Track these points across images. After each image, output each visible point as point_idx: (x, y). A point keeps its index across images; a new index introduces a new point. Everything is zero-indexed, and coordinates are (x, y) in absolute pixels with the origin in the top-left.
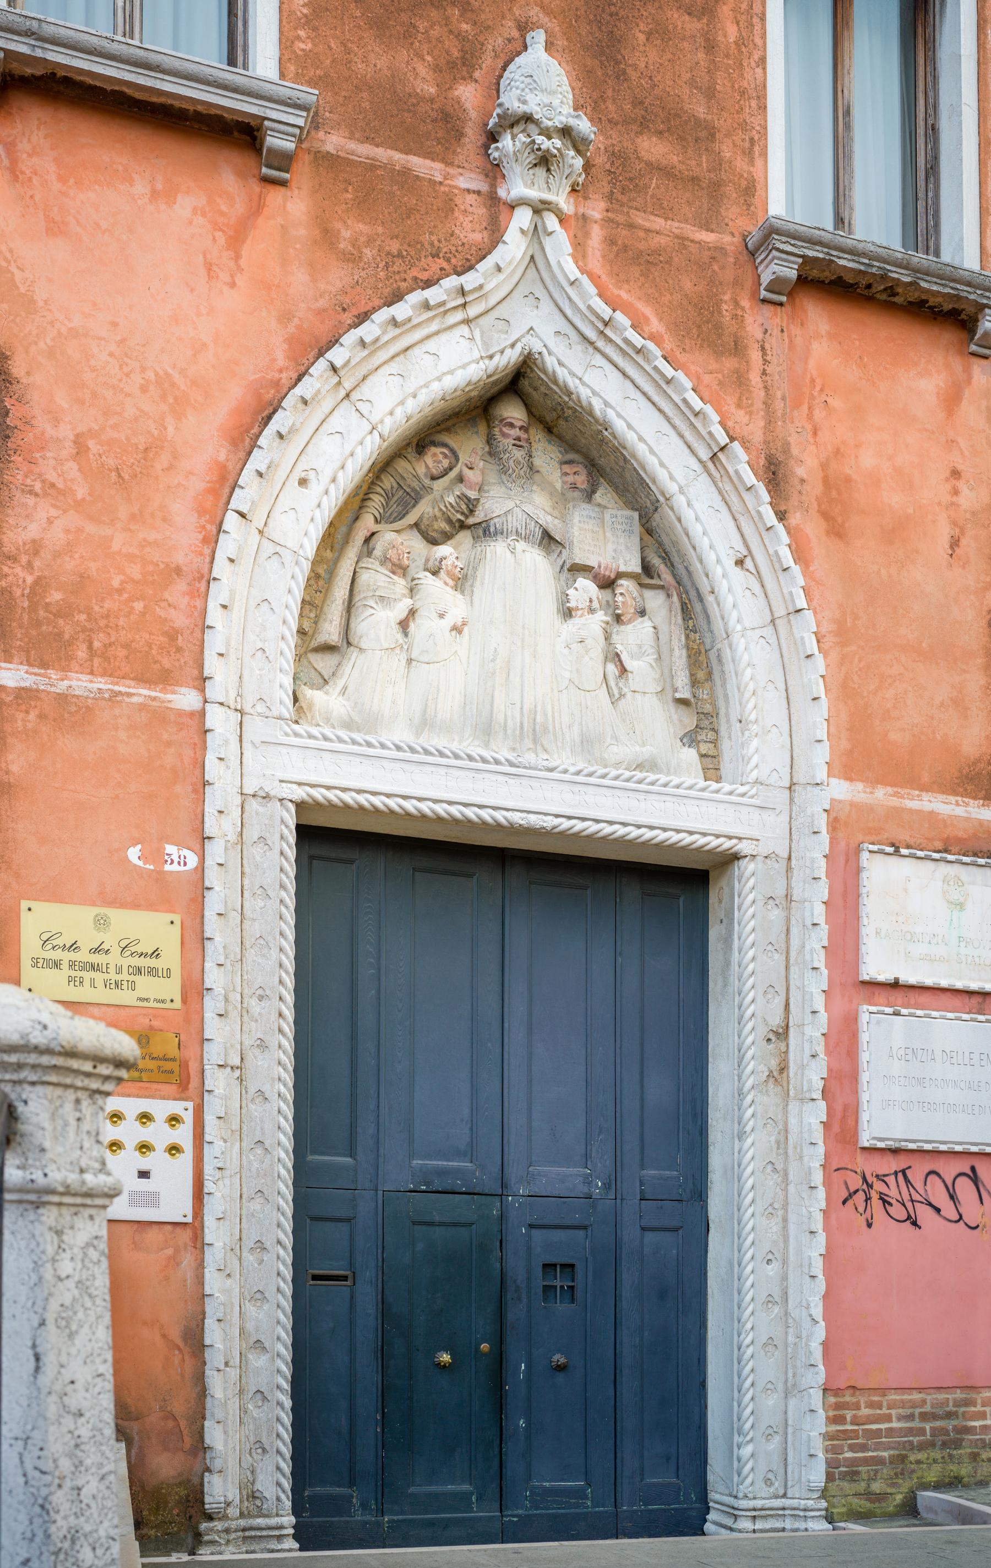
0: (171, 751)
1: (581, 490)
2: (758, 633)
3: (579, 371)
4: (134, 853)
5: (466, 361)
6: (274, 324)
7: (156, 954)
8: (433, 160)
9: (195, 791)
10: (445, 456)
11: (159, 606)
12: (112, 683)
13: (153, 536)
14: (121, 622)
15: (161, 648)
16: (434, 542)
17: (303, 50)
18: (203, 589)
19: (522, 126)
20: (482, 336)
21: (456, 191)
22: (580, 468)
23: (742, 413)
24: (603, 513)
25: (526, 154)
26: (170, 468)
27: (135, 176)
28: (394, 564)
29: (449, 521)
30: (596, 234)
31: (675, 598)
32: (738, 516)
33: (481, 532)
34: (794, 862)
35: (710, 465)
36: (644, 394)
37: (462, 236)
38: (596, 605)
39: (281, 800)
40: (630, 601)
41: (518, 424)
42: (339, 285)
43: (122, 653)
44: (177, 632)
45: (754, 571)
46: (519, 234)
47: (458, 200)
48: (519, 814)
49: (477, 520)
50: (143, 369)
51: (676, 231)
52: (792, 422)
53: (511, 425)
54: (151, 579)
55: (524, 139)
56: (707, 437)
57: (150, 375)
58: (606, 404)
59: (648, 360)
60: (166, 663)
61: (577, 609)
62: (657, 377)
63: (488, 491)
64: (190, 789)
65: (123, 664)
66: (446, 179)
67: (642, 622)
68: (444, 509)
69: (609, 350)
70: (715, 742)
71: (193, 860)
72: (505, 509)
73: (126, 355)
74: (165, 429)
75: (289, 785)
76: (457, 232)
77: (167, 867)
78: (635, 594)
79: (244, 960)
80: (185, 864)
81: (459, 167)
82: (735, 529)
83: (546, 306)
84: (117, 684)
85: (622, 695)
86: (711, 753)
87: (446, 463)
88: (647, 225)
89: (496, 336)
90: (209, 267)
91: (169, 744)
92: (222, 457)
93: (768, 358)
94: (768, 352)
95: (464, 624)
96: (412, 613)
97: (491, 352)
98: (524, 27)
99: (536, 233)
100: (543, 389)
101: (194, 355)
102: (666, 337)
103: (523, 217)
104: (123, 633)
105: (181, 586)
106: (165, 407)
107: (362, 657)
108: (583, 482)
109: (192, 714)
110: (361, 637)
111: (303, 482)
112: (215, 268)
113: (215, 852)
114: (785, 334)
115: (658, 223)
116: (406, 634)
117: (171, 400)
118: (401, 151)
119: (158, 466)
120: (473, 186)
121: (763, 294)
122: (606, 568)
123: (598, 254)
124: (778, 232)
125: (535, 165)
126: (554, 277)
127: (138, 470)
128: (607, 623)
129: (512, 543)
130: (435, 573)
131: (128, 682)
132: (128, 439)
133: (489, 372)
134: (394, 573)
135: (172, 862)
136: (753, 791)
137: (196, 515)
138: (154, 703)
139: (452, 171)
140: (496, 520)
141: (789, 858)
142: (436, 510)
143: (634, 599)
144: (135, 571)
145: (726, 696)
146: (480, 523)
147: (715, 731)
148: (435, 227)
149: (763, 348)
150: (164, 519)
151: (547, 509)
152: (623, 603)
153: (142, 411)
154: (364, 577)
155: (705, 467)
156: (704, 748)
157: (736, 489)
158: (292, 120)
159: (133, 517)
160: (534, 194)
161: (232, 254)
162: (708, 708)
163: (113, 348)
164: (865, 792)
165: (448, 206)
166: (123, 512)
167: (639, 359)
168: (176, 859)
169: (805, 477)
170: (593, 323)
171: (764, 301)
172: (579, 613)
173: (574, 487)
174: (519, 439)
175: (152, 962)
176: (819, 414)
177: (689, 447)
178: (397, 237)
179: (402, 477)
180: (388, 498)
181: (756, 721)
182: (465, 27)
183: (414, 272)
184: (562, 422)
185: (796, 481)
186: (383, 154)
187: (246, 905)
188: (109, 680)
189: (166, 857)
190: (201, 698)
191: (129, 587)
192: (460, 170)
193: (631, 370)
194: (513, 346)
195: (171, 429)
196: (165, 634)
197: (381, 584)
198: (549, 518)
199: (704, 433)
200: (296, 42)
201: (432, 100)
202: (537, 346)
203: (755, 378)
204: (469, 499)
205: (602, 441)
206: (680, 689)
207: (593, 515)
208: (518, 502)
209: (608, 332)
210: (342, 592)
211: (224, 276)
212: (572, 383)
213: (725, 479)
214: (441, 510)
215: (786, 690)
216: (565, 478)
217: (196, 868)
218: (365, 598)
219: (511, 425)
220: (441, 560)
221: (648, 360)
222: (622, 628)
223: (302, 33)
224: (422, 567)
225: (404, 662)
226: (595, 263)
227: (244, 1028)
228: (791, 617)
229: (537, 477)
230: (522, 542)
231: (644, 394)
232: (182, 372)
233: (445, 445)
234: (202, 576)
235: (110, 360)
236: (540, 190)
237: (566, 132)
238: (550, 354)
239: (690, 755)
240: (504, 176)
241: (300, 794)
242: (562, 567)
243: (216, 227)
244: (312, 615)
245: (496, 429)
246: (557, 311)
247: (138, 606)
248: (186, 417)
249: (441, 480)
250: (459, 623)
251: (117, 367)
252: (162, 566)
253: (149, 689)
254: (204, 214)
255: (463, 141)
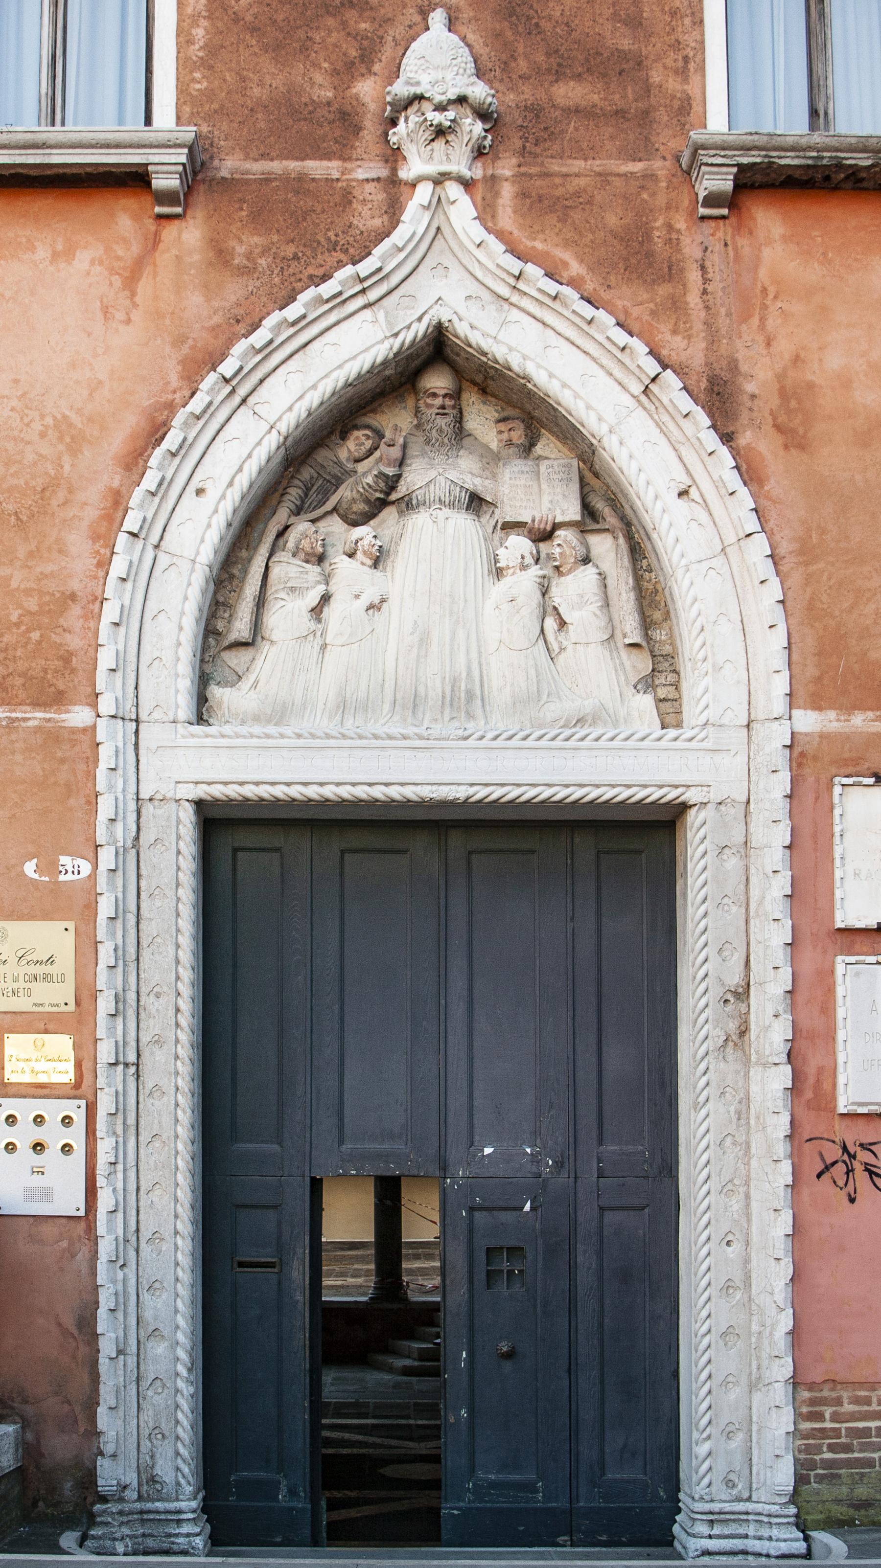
0: (65, 767)
1: (517, 446)
2: (706, 565)
3: (492, 330)
4: (30, 868)
5: (369, 344)
6: (168, 349)
7: (50, 960)
8: (330, 159)
9: (89, 803)
10: (368, 437)
11: (55, 633)
12: (10, 711)
13: (49, 568)
14: (19, 653)
15: (56, 671)
16: (355, 524)
17: (198, 90)
18: (97, 610)
19: (415, 106)
20: (386, 317)
21: (354, 184)
22: (517, 424)
23: (678, 338)
24: (538, 465)
25: (421, 132)
26: (66, 503)
27: (36, 244)
28: (307, 554)
29: (367, 501)
30: (507, 191)
31: (621, 540)
32: (677, 446)
33: (404, 506)
34: (752, 805)
35: (643, 398)
36: (567, 339)
37: (360, 225)
38: (529, 560)
39: (177, 801)
40: (568, 551)
41: (443, 392)
42: (233, 298)
43: (19, 681)
44: (72, 654)
45: (699, 500)
46: (420, 210)
47: (356, 192)
48: (429, 787)
49: (400, 495)
50: (42, 417)
51: (597, 169)
52: (740, 337)
53: (434, 395)
54: (47, 608)
55: (417, 119)
56: (637, 371)
57: (49, 421)
58: (525, 357)
59: (565, 305)
60: (61, 685)
61: (508, 568)
62: (577, 320)
63: (411, 465)
64: (83, 801)
65: (20, 692)
66: (343, 174)
67: (584, 571)
68: (362, 490)
69: (525, 303)
70: (676, 686)
71: (86, 868)
72: (427, 480)
73: (27, 407)
74: (62, 467)
75: (186, 785)
76: (355, 222)
77: (62, 878)
78: (575, 542)
79: (141, 959)
80: (79, 873)
81: (357, 160)
82: (677, 460)
83: (456, 273)
84: (14, 711)
85: (562, 649)
86: (670, 696)
87: (368, 444)
88: (564, 170)
89: (401, 313)
90: (106, 311)
91: (63, 761)
92: (116, 483)
93: (710, 276)
94: (710, 270)
95: (383, 601)
96: (326, 598)
97: (396, 330)
98: (424, 13)
99: (438, 204)
100: (462, 353)
101: (90, 394)
102: (587, 278)
103: (424, 192)
104: (20, 663)
105: (76, 610)
106: (61, 447)
107: (274, 649)
108: (520, 437)
109: (84, 730)
110: (272, 630)
111: (200, 492)
112: (111, 310)
113: (106, 858)
114: (730, 248)
115: (578, 165)
116: (319, 620)
117: (68, 440)
118: (297, 159)
119: (54, 503)
120: (373, 175)
121: (702, 211)
122: (541, 522)
123: (509, 210)
124: (704, 147)
125: (433, 140)
126: (461, 244)
127: (35, 510)
128: (544, 577)
129: (434, 513)
130: (351, 555)
131: (24, 708)
132: (27, 483)
133: (395, 350)
134: (307, 562)
135: (67, 872)
136: (702, 735)
137: (90, 542)
138: (49, 725)
139: (348, 165)
140: (418, 492)
141: (748, 802)
142: (355, 492)
143: (574, 548)
144: (32, 604)
145: (680, 634)
146: (402, 498)
147: (675, 671)
148: (332, 223)
149: (703, 268)
150: (60, 551)
151: (474, 471)
152: (561, 554)
153: (41, 455)
154: (276, 571)
155: (638, 401)
156: (662, 693)
157: (673, 418)
158: (173, 159)
159: (31, 555)
160: (432, 169)
161: (127, 293)
162: (667, 649)
163: (14, 403)
164: (838, 720)
165: (347, 198)
166: (21, 553)
167: (556, 305)
168: (70, 870)
169: (757, 392)
170: (503, 280)
171: (703, 218)
172: (511, 571)
173: (509, 443)
174: (443, 407)
175: (48, 969)
176: (772, 323)
177: (620, 384)
178: (292, 241)
179: (323, 466)
180: (307, 491)
181: (705, 660)
182: (363, 26)
183: (311, 270)
184: (490, 382)
185: (745, 399)
186: (276, 166)
187: (143, 905)
188: (7, 708)
189: (61, 868)
190: (94, 714)
191: (26, 619)
192: (359, 163)
193: (550, 318)
194: (420, 319)
195: (67, 467)
196: (61, 658)
197: (291, 575)
198: (478, 481)
199: (633, 367)
200: (192, 85)
201: (329, 104)
202: (444, 314)
203: (694, 299)
204: (386, 476)
205: (529, 394)
206: (629, 634)
207: (525, 469)
208: (441, 471)
209: (521, 285)
210: (253, 589)
211: (120, 316)
212: (486, 344)
213: (661, 410)
214: (358, 491)
215: (742, 621)
216: (500, 437)
217: (90, 876)
218: (276, 591)
219: (434, 395)
220: (357, 542)
221: (565, 305)
222: (562, 579)
223: (197, 75)
224: (341, 551)
225: (317, 648)
226: (506, 219)
227: (141, 1025)
228: (742, 543)
229: (466, 442)
230: (447, 510)
231: (567, 339)
232: (79, 412)
233: (368, 427)
234: (96, 598)
235: (11, 414)
236: (441, 162)
237: (462, 100)
238: (460, 320)
239: (646, 702)
240: (405, 158)
241: (201, 792)
242: (495, 527)
243: (112, 271)
244: (226, 615)
245: (421, 402)
246: (468, 275)
247: (35, 636)
248: (82, 453)
249: (366, 461)
250: (377, 602)
251: (18, 420)
252: (58, 595)
253: (45, 712)
254: (101, 263)
255: (361, 134)
